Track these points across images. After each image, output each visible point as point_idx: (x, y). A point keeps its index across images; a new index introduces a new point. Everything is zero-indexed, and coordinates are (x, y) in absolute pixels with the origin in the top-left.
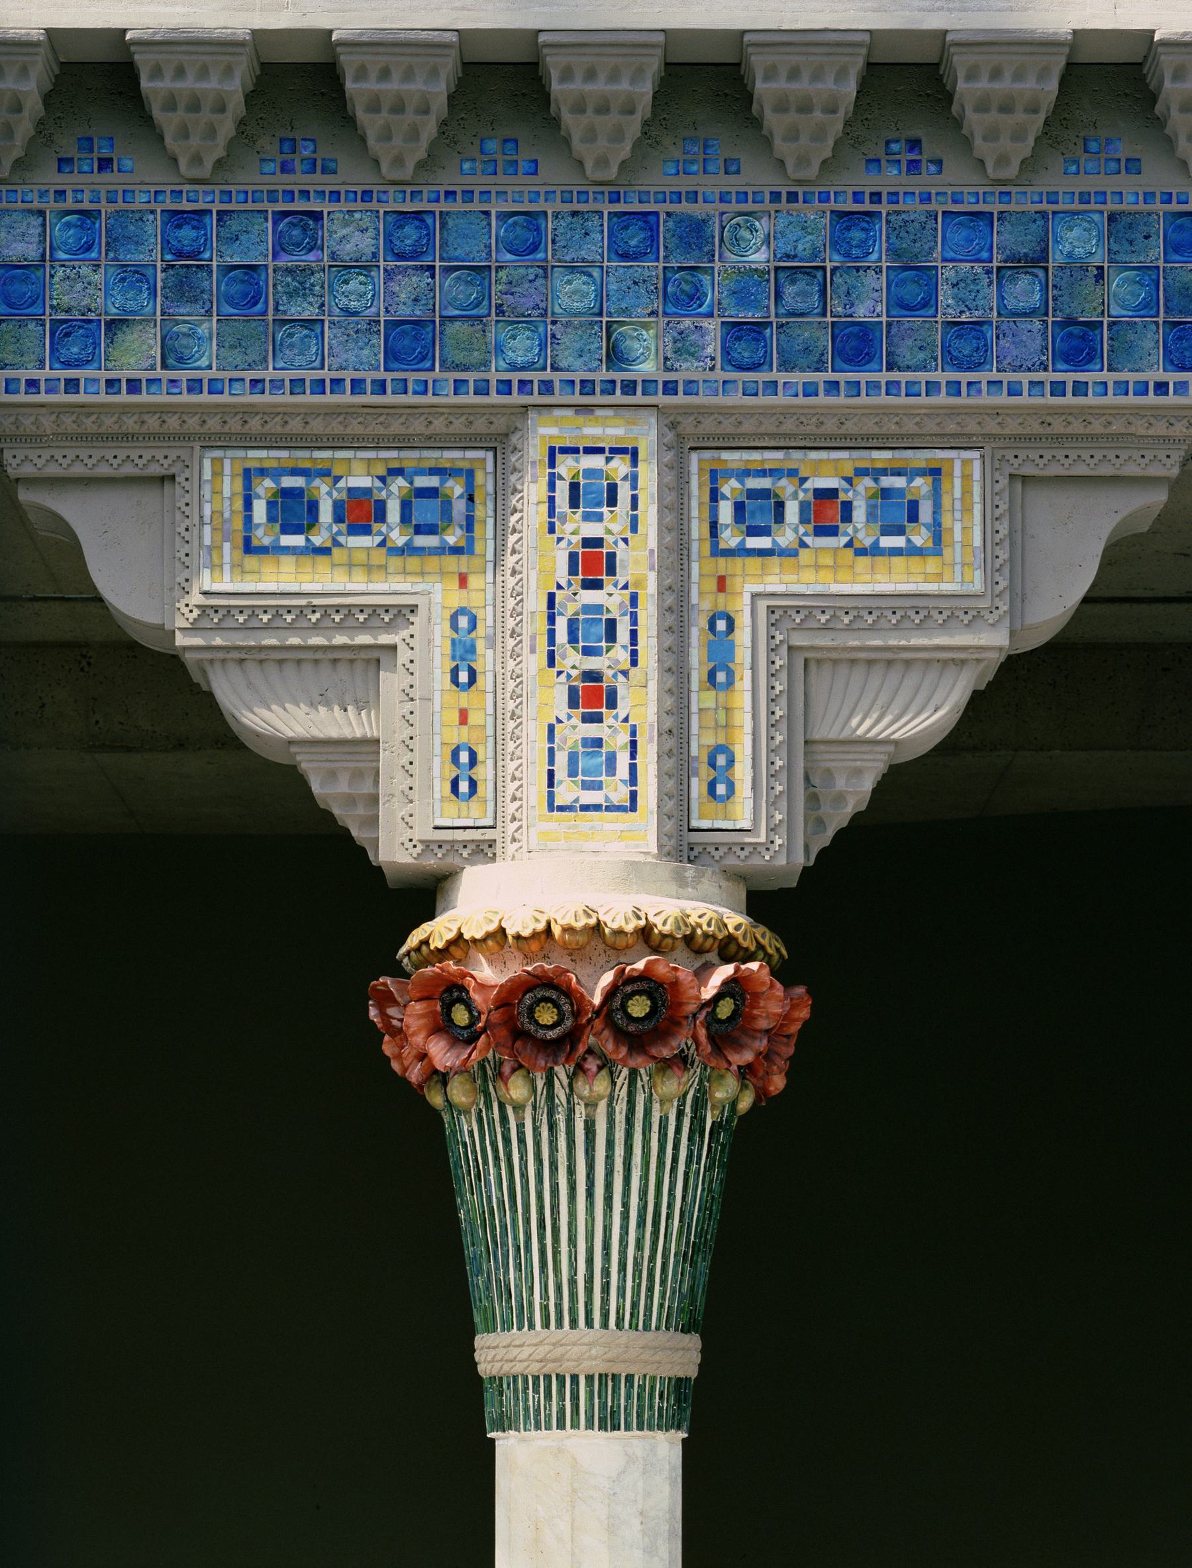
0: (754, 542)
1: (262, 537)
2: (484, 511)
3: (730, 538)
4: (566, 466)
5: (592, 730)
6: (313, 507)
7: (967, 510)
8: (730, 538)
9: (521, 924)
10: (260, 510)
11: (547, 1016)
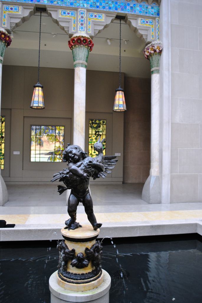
1: (62, 14)
2: (76, 14)
3: (90, 17)
4: (81, 12)
6: (66, 13)
8: (90, 17)
10: (62, 13)
11: (79, 41)
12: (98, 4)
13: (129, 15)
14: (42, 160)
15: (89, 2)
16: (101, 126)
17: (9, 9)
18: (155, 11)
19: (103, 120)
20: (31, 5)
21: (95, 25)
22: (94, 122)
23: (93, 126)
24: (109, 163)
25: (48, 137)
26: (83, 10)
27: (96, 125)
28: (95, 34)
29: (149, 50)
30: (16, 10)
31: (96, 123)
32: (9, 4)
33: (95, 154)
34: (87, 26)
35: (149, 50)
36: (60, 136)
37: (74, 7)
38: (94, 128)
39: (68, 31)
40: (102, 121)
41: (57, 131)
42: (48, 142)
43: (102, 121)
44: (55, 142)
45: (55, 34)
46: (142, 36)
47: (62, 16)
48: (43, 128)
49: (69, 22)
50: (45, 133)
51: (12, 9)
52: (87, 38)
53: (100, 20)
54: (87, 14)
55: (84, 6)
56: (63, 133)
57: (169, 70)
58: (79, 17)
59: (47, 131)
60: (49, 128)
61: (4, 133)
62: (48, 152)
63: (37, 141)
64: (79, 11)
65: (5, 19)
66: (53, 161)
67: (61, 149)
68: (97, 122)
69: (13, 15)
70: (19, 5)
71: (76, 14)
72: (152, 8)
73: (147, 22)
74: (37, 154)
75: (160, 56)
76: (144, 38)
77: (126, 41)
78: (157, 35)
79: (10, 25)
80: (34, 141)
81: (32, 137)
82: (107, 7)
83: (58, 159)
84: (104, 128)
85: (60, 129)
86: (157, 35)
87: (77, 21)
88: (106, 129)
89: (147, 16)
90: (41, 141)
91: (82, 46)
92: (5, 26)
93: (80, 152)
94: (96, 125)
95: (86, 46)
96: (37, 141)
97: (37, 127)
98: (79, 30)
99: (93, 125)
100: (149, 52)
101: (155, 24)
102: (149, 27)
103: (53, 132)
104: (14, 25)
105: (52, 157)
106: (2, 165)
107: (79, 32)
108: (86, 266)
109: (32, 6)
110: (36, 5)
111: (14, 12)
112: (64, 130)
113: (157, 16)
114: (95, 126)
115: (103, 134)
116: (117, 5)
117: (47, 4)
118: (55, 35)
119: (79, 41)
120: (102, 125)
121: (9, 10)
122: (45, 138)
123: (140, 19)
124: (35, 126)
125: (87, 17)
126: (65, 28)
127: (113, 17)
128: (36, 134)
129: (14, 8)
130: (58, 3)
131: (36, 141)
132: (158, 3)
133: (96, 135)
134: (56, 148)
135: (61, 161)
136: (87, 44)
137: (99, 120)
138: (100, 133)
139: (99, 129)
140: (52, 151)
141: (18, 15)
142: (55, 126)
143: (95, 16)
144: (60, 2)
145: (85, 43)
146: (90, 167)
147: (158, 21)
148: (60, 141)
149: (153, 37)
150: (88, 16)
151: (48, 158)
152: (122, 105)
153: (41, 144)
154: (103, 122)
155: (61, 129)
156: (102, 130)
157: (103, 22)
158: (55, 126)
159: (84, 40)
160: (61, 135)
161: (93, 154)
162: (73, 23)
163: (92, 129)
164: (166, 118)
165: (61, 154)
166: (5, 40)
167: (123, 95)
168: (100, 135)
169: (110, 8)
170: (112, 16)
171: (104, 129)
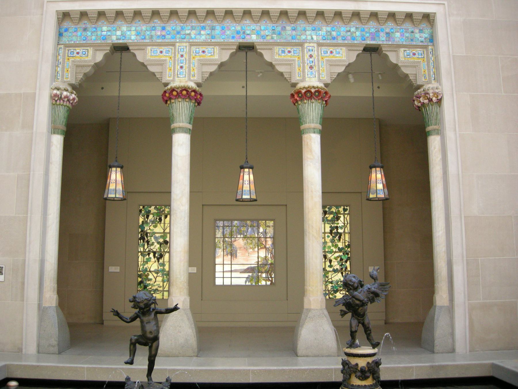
0: (325, 55)
4: (308, 48)
5: (311, 70)
6: (285, 51)
7: (344, 52)
9: (307, 86)
11: (308, 94)
12: (334, 34)
13: (383, 45)
14: (235, 282)
15: (320, 32)
16: (340, 217)
17: (200, 52)
18: (426, 36)
19: (344, 206)
20: (232, 44)
21: (331, 65)
22: (327, 210)
23: (327, 217)
24: (382, 289)
25: (245, 241)
26: (312, 45)
27: (332, 216)
28: (331, 80)
29: (421, 100)
30: (210, 53)
31: (332, 213)
32: (200, 45)
33: (331, 269)
34: (319, 69)
35: (421, 100)
36: (266, 238)
37: (297, 41)
38: (328, 221)
39: (290, 77)
40: (342, 207)
41: (261, 230)
42: (246, 249)
43: (342, 207)
44: (258, 249)
45: (261, 72)
46: (407, 76)
47: (279, 56)
48: (236, 224)
49: (290, 65)
50: (241, 234)
51: (204, 52)
52: (321, 88)
53: (338, 57)
54: (318, 50)
55: (312, 38)
56: (272, 232)
57: (455, 130)
58: (307, 56)
59: (243, 229)
60: (246, 224)
61: (168, 235)
62: (246, 267)
63: (226, 248)
64: (306, 46)
65: (195, 68)
66: (256, 283)
67: (270, 262)
68: (334, 210)
69: (207, 60)
70: (215, 45)
71: (301, 52)
72: (421, 31)
73: (414, 54)
74: (226, 272)
75: (440, 107)
76: (410, 79)
77: (380, 74)
78: (432, 73)
79: (202, 75)
80: (220, 248)
81: (216, 241)
82: (349, 37)
83: (264, 280)
84: (347, 219)
85: (265, 225)
86: (432, 73)
87: (303, 62)
88: (350, 223)
89: (414, 44)
90: (233, 248)
91: (313, 101)
92: (195, 78)
93: (358, 280)
94: (332, 216)
95: (320, 101)
96: (226, 248)
97: (225, 222)
98: (306, 76)
99: (327, 216)
100: (420, 102)
101: (428, 56)
102: (419, 62)
103: (254, 232)
104: (208, 76)
105: (252, 277)
106: (166, 291)
107: (307, 79)
108: (368, 377)
109: (233, 45)
110: (240, 43)
111: (207, 56)
112: (274, 226)
113: (430, 44)
114: (329, 218)
115: (344, 232)
116: (364, 33)
117: (256, 41)
118: (261, 74)
119: (308, 94)
120: (342, 216)
121: (201, 53)
122: (239, 242)
123: (402, 50)
124: (222, 222)
125: (318, 55)
126: (284, 74)
127: (360, 50)
128: (223, 236)
129: (206, 50)
130: (272, 38)
131: (225, 248)
132: (430, 23)
133: (331, 235)
134: (260, 260)
135: (269, 283)
136: (321, 97)
137: (337, 207)
138: (340, 231)
139: (338, 223)
140: (252, 266)
141: (213, 60)
142: (256, 222)
143: (331, 52)
144: (275, 36)
145: (317, 97)
146: (369, 293)
147: (432, 51)
148: (267, 246)
149: (425, 77)
150: (320, 54)
151: (245, 279)
152: (381, 190)
153: (233, 254)
154: (345, 210)
155: (268, 224)
156: (343, 225)
157: (344, 61)
158: (258, 220)
159: (316, 92)
160: (268, 236)
161: (328, 269)
162: (297, 66)
163: (324, 224)
164: (454, 210)
165: (269, 270)
166: (196, 100)
167: (383, 174)
168: (340, 234)
169: (354, 39)
170: (357, 50)
171: (346, 222)
